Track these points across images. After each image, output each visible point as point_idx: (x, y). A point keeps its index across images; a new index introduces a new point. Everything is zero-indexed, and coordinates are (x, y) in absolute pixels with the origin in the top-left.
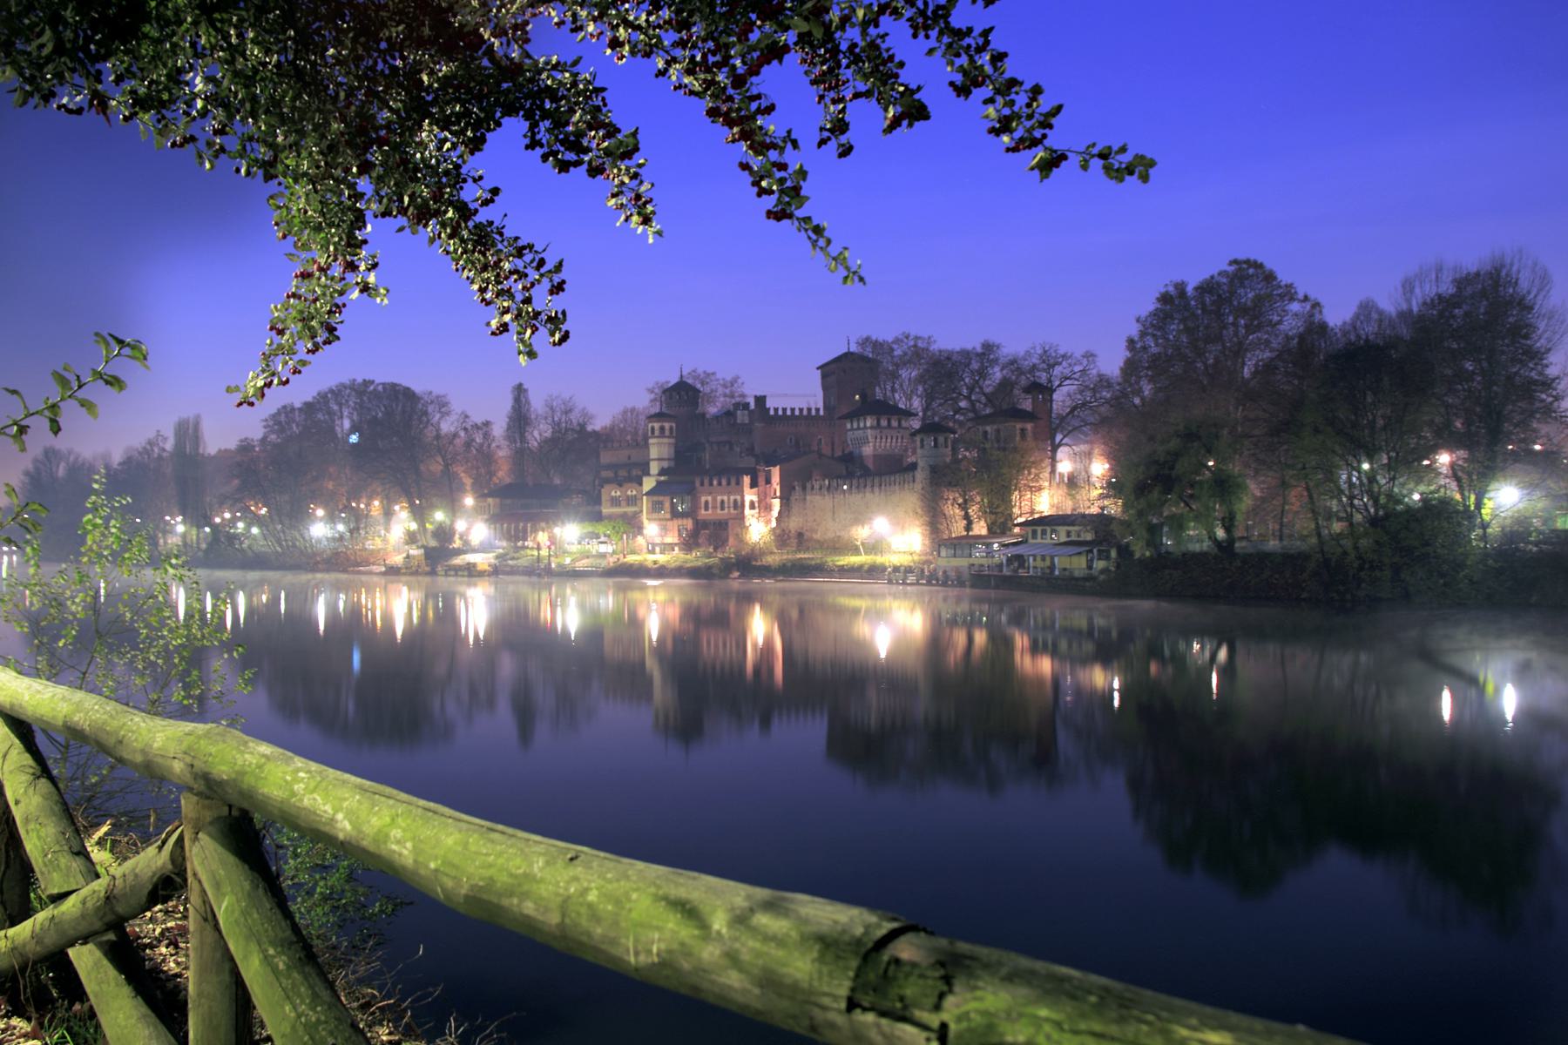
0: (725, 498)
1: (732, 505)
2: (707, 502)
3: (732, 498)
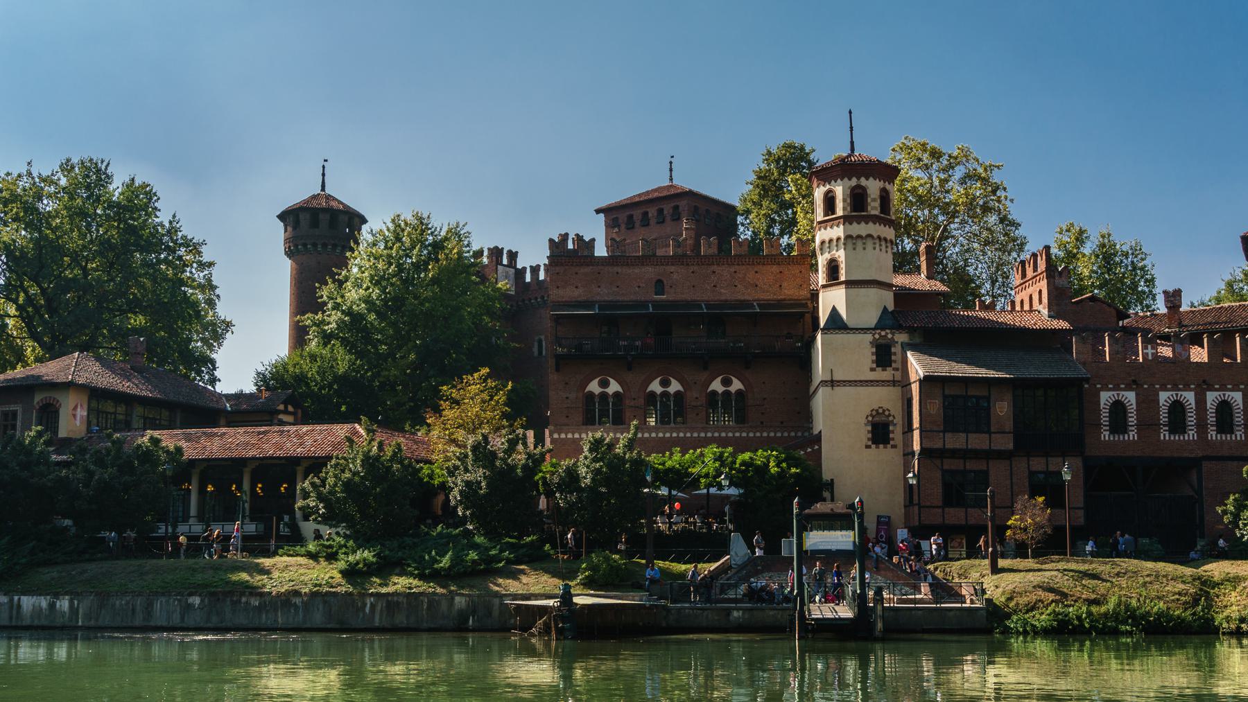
1: (1211, 418)
2: (1118, 408)
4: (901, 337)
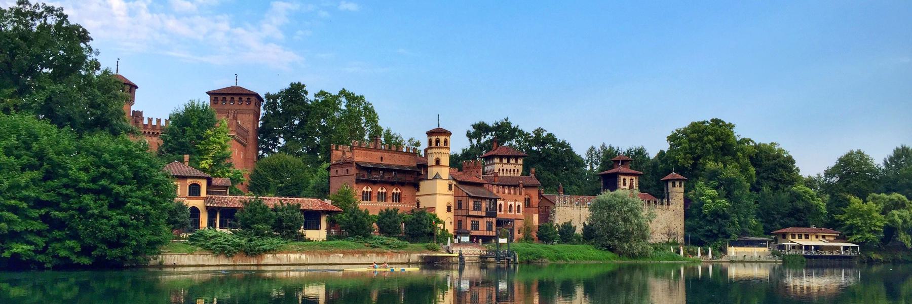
0: (513, 203)
1: (517, 209)
2: (500, 205)
3: (517, 204)
4: (454, 183)
